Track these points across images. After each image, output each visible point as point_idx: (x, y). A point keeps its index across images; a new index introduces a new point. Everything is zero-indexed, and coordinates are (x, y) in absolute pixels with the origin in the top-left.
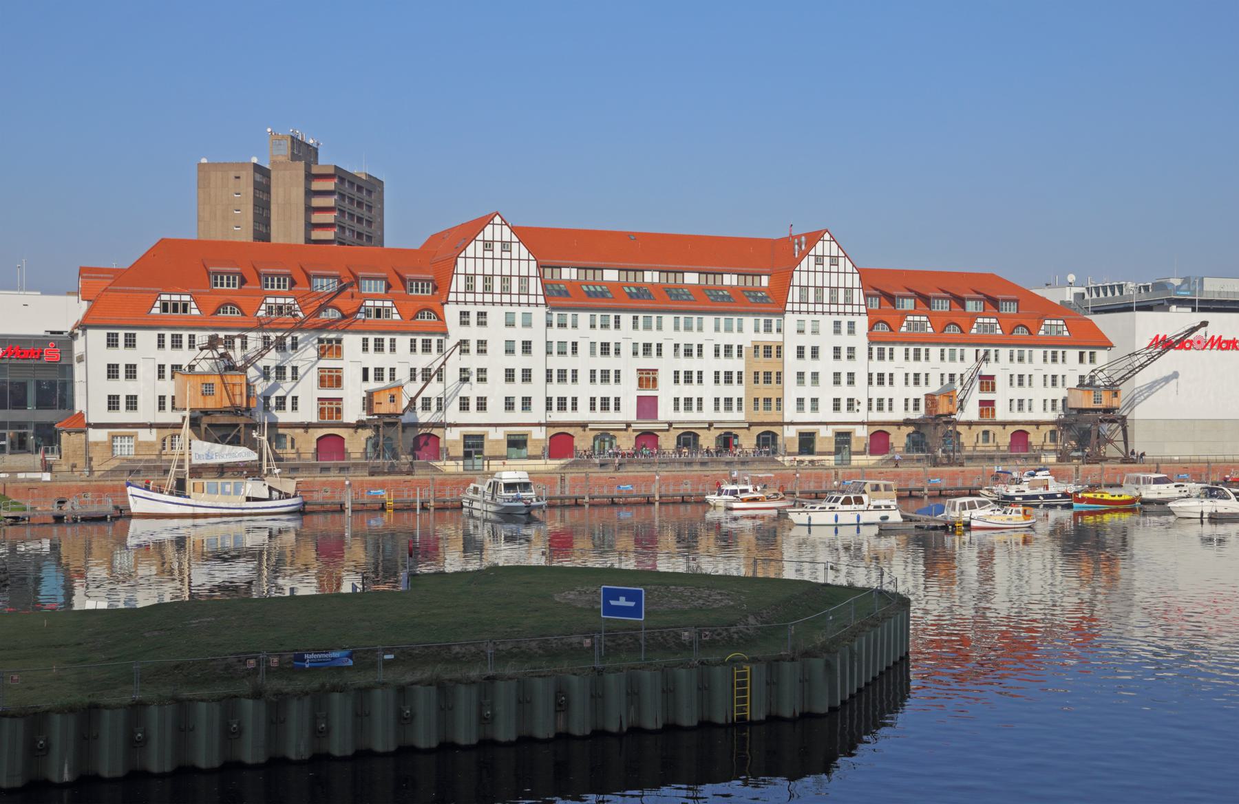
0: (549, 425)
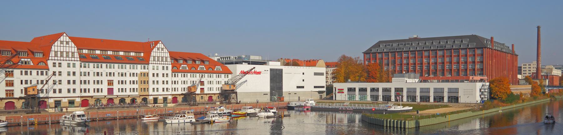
0: (81, 97)
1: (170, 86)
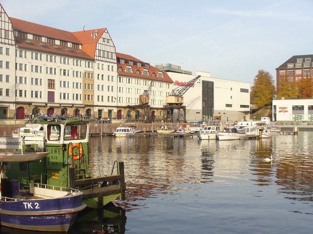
0: (16, 103)
1: (114, 94)
